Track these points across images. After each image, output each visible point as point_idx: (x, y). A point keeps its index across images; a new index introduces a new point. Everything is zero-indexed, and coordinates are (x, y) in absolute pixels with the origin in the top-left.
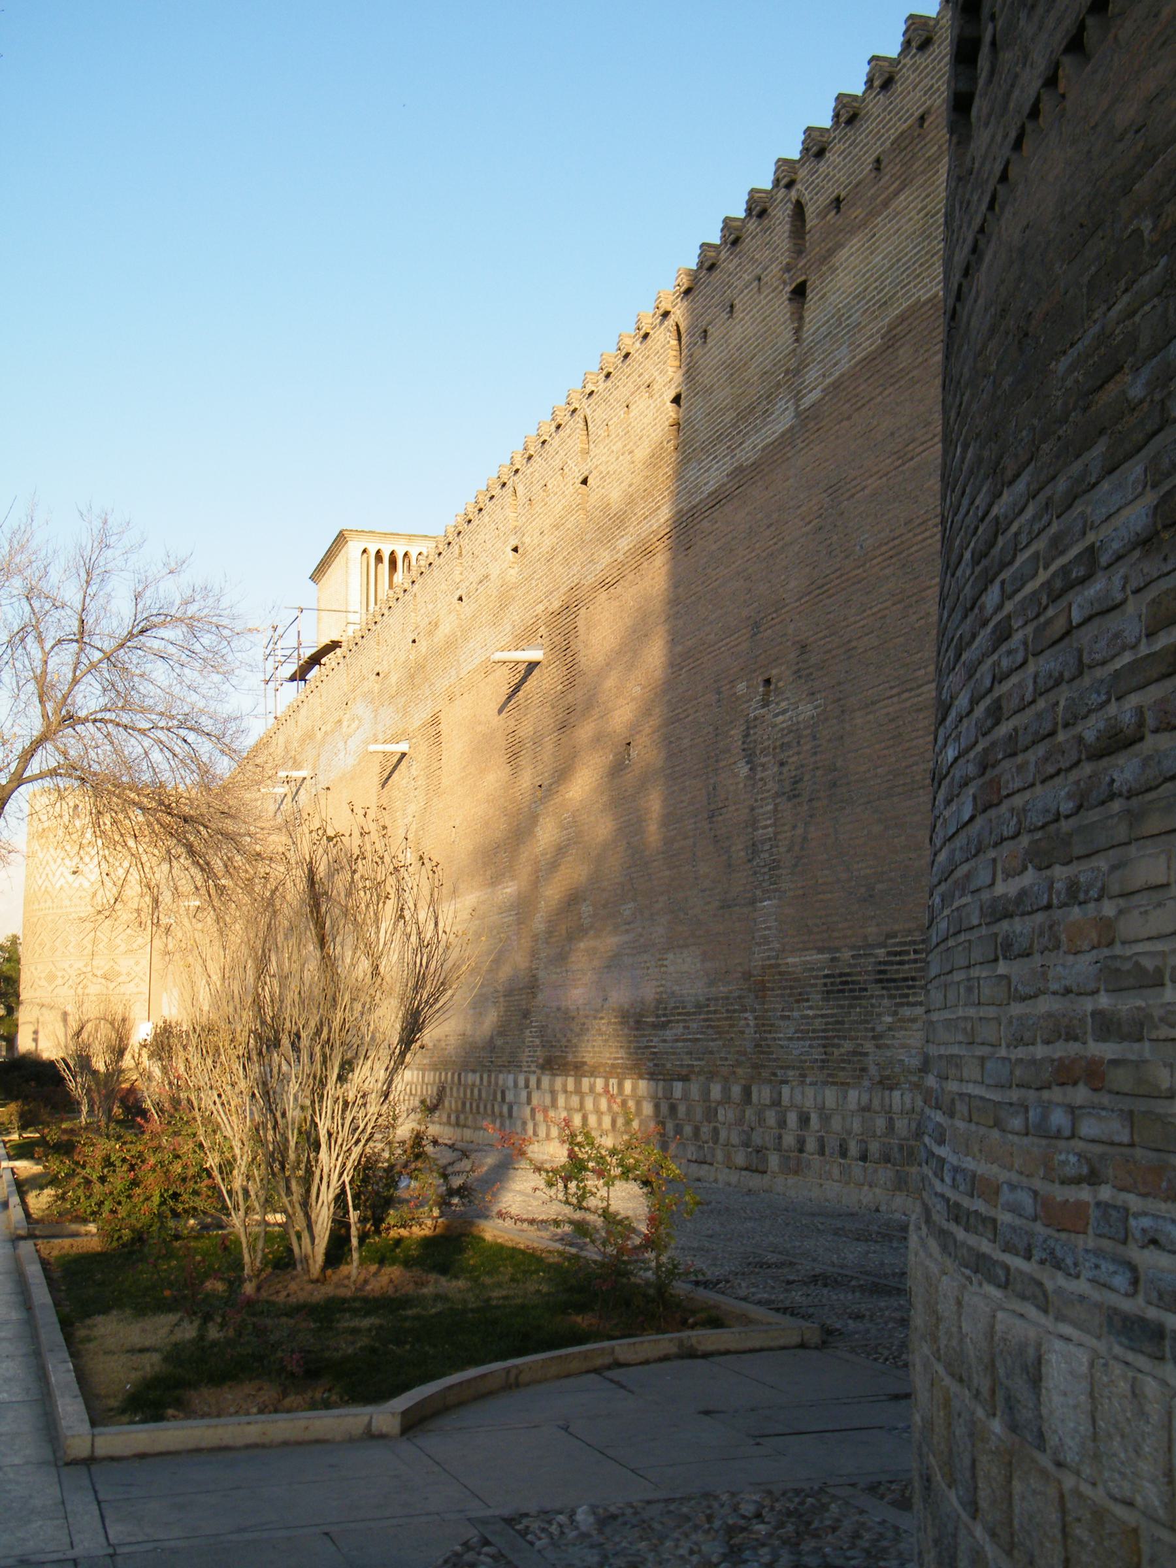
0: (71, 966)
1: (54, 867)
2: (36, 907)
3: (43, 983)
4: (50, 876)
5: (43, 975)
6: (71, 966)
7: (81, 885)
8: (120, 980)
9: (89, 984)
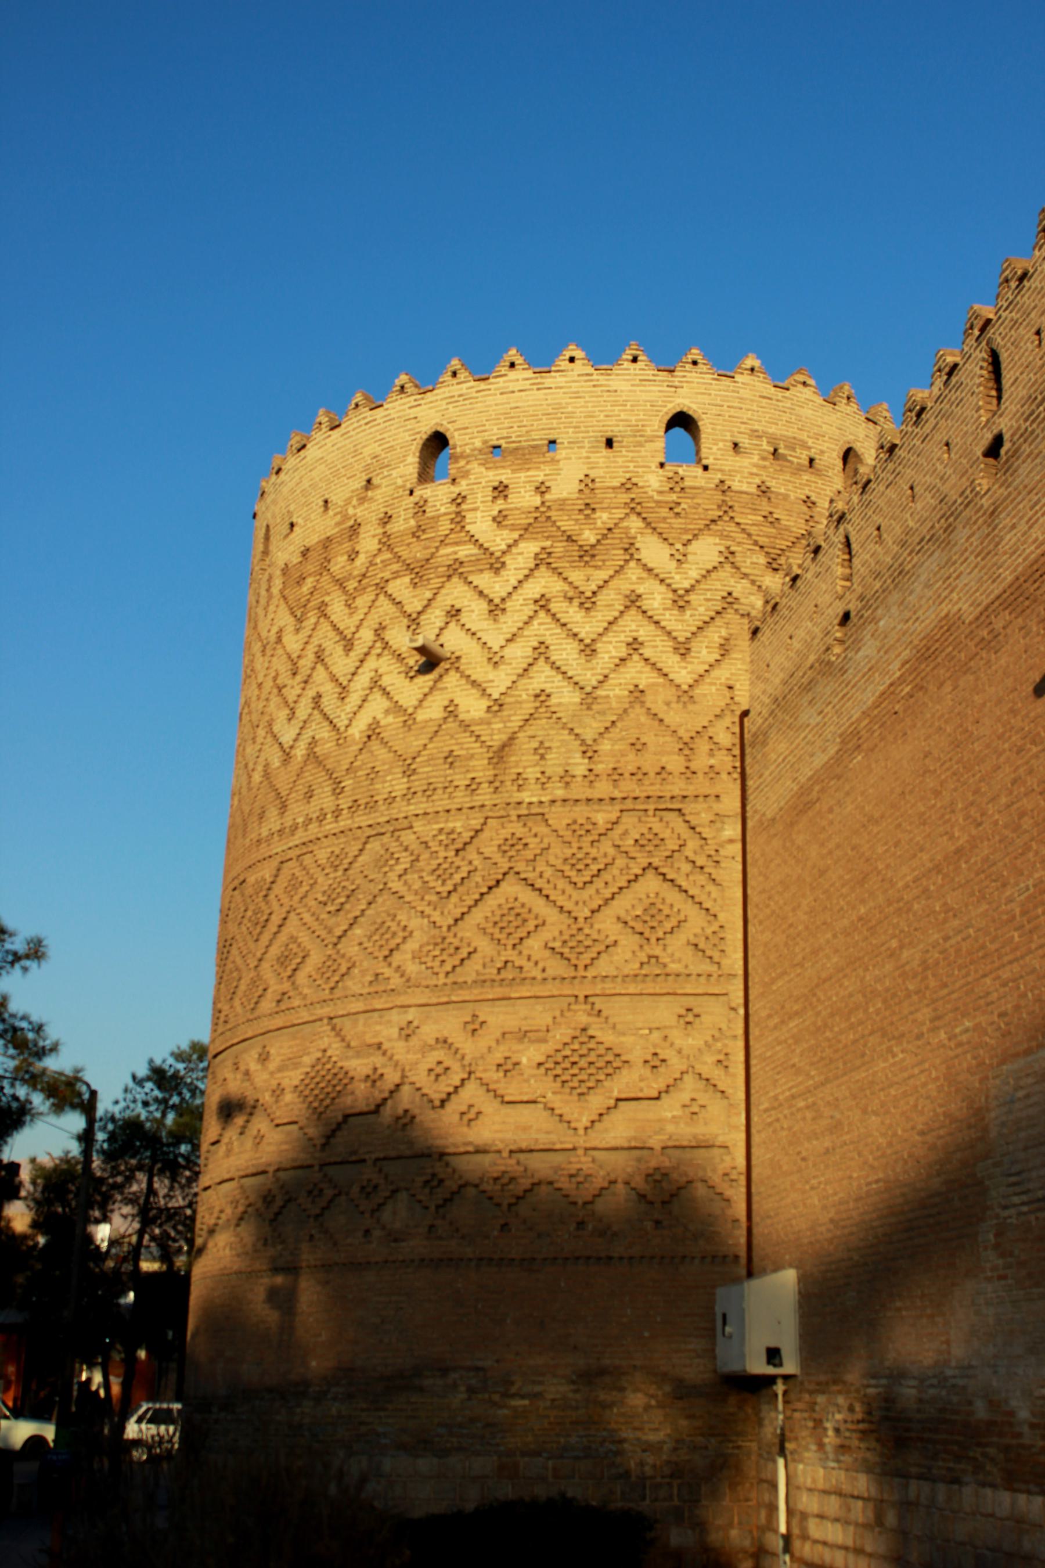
0: (407, 1032)
1: (341, 663)
2: (273, 822)
4: (329, 702)
6: (407, 1032)
7: (451, 711)
8: (618, 1086)
9: (489, 1106)
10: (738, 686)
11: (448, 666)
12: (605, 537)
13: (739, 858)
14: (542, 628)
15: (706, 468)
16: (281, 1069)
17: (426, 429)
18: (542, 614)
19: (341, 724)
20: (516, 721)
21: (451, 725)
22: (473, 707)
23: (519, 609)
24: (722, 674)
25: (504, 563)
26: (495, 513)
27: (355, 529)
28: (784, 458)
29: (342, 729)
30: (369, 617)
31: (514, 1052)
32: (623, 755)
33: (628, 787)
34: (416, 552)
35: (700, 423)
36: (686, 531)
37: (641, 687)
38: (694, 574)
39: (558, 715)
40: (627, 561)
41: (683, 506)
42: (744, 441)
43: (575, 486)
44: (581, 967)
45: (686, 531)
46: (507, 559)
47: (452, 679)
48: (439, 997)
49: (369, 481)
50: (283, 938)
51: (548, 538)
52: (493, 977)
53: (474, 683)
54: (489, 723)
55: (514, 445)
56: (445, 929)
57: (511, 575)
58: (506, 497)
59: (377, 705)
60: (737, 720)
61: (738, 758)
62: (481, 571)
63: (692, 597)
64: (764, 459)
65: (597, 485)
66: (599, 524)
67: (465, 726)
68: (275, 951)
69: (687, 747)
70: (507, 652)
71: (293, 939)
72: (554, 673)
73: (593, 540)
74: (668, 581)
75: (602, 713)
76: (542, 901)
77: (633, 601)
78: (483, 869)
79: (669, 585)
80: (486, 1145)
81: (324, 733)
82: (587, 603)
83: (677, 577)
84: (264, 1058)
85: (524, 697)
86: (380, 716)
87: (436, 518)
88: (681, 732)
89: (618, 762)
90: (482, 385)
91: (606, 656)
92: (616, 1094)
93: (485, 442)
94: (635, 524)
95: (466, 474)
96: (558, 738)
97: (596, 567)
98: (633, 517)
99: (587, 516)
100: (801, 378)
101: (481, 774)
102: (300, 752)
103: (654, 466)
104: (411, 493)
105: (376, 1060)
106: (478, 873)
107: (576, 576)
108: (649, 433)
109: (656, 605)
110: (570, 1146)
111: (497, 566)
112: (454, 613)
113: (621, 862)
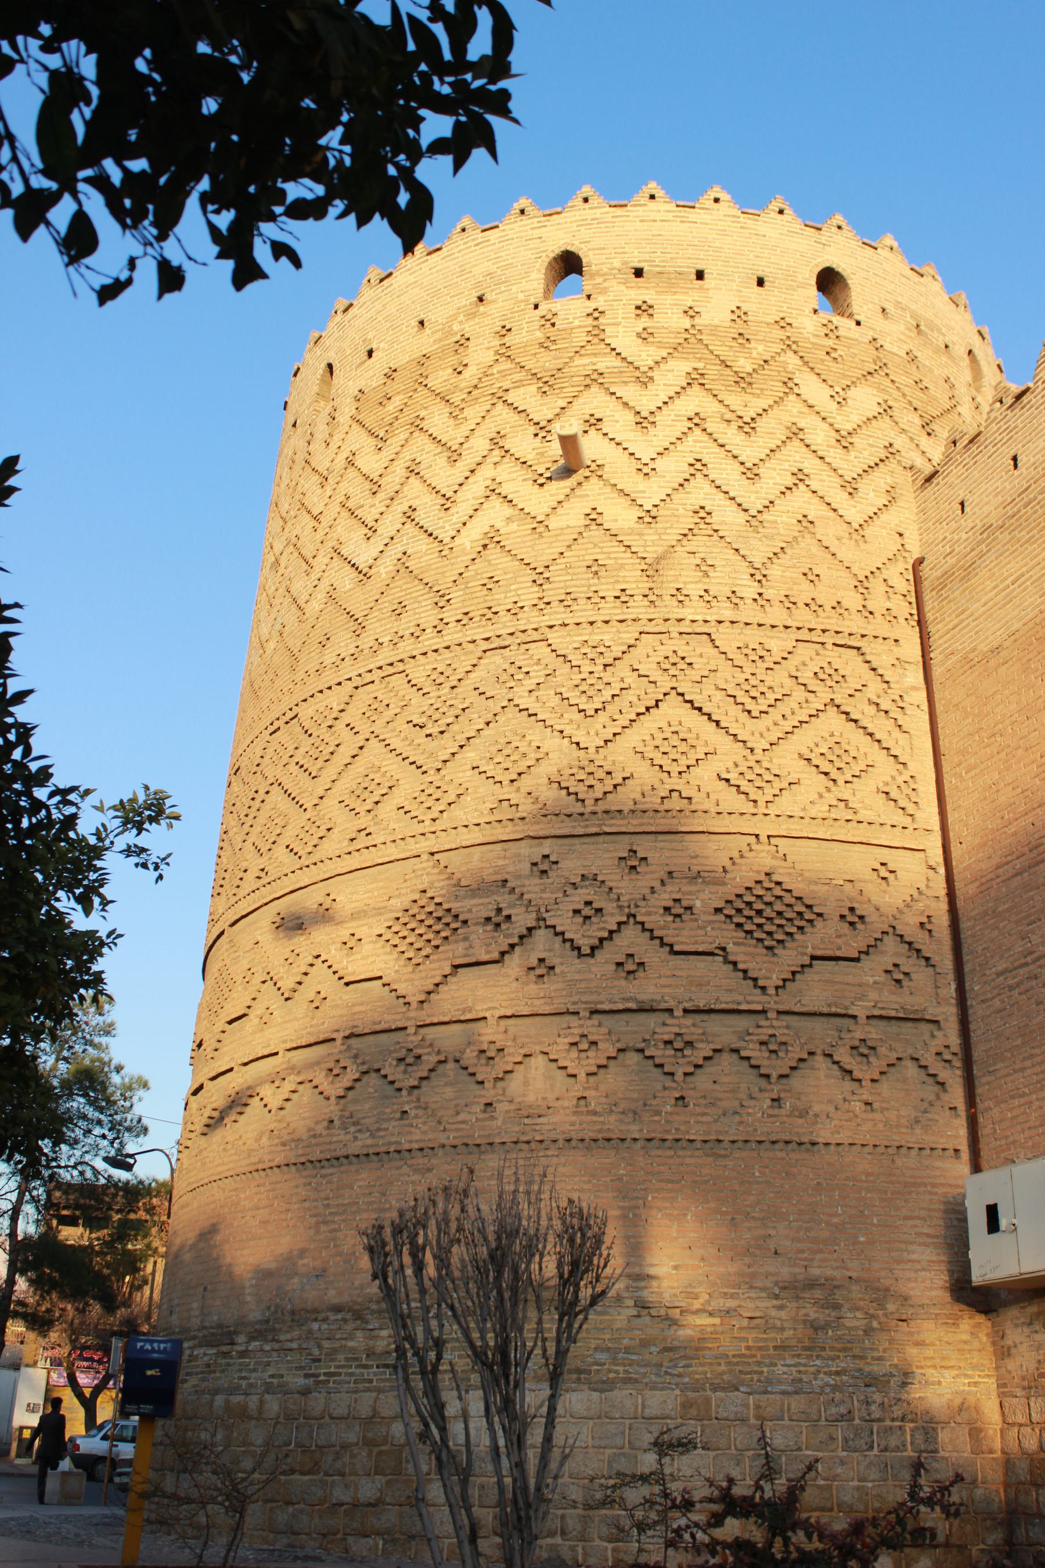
7: (593, 518)
10: (906, 535)
11: (588, 474)
13: (925, 706)
15: (858, 323)
17: (555, 248)
18: (697, 431)
19: (445, 536)
20: (672, 537)
21: (595, 533)
24: (892, 519)
25: (651, 378)
26: (640, 329)
27: (463, 342)
28: (925, 335)
29: (447, 540)
30: (483, 426)
31: (684, 894)
32: (795, 583)
33: (802, 616)
34: (546, 362)
35: (849, 282)
37: (810, 518)
38: (856, 419)
39: (721, 533)
41: (839, 352)
42: (889, 307)
44: (761, 803)
45: (845, 376)
46: (655, 374)
47: (594, 484)
48: (587, 826)
49: (481, 299)
51: (700, 359)
52: (657, 807)
54: (641, 534)
55: (658, 269)
56: (592, 750)
59: (496, 513)
60: (910, 567)
61: (914, 605)
63: (854, 439)
64: (910, 330)
65: (750, 318)
66: (754, 354)
69: (862, 585)
70: (660, 464)
72: (715, 490)
74: (829, 420)
75: (771, 538)
77: (795, 433)
78: (638, 688)
79: (831, 425)
80: (652, 1000)
81: (420, 545)
82: (748, 427)
83: (839, 418)
85: (681, 511)
88: (855, 569)
89: (791, 589)
90: (619, 211)
91: (771, 482)
92: (810, 950)
93: (624, 263)
94: (792, 360)
95: (604, 291)
96: (720, 556)
98: (790, 354)
100: (932, 272)
101: (634, 586)
102: (385, 568)
103: (808, 310)
104: (536, 307)
105: (499, 899)
106: (631, 692)
107: (735, 400)
108: (800, 279)
109: (819, 441)
110: (759, 1007)
111: (644, 381)
112: (594, 422)
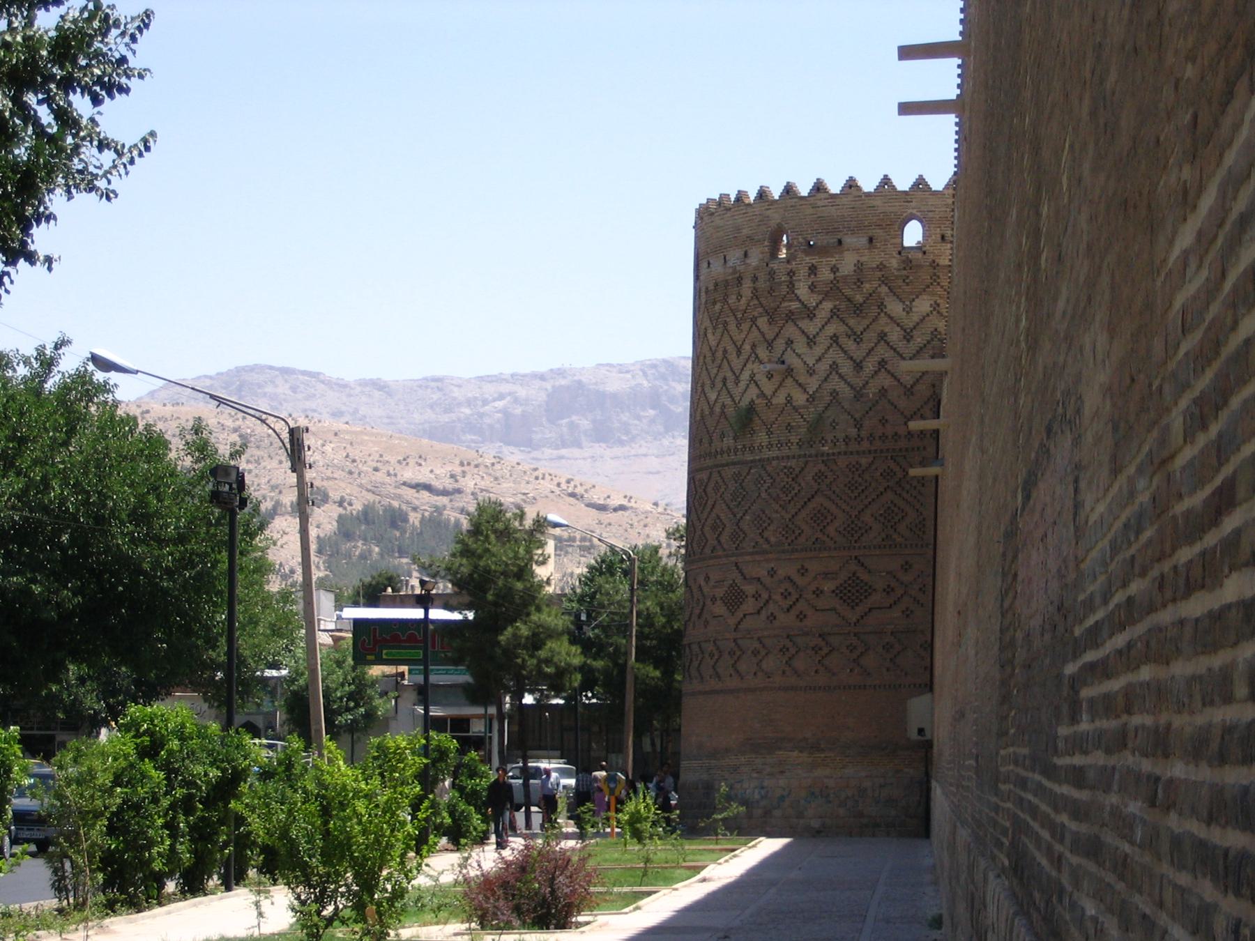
3: (719, 609)
5: (720, 592)
6: (772, 572)
7: (789, 400)
12: (868, 299)
14: (834, 355)
16: (714, 587)
18: (834, 345)
19: (737, 399)
22: (800, 398)
23: (823, 341)
27: (739, 280)
36: (911, 293)
40: (879, 314)
43: (852, 268)
45: (911, 293)
50: (713, 515)
53: (800, 385)
57: (818, 322)
58: (815, 275)
62: (803, 318)
67: (796, 409)
68: (710, 521)
71: (718, 517)
73: (861, 300)
76: (834, 507)
77: (882, 336)
81: (728, 401)
82: (858, 339)
84: (707, 579)
86: (755, 398)
87: (780, 283)
94: (884, 289)
97: (863, 317)
98: (883, 286)
99: (859, 287)
102: (717, 409)
113: (873, 484)
